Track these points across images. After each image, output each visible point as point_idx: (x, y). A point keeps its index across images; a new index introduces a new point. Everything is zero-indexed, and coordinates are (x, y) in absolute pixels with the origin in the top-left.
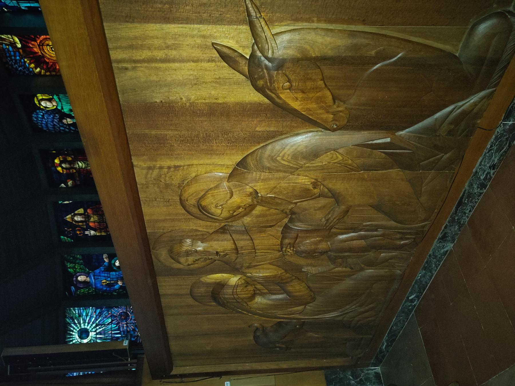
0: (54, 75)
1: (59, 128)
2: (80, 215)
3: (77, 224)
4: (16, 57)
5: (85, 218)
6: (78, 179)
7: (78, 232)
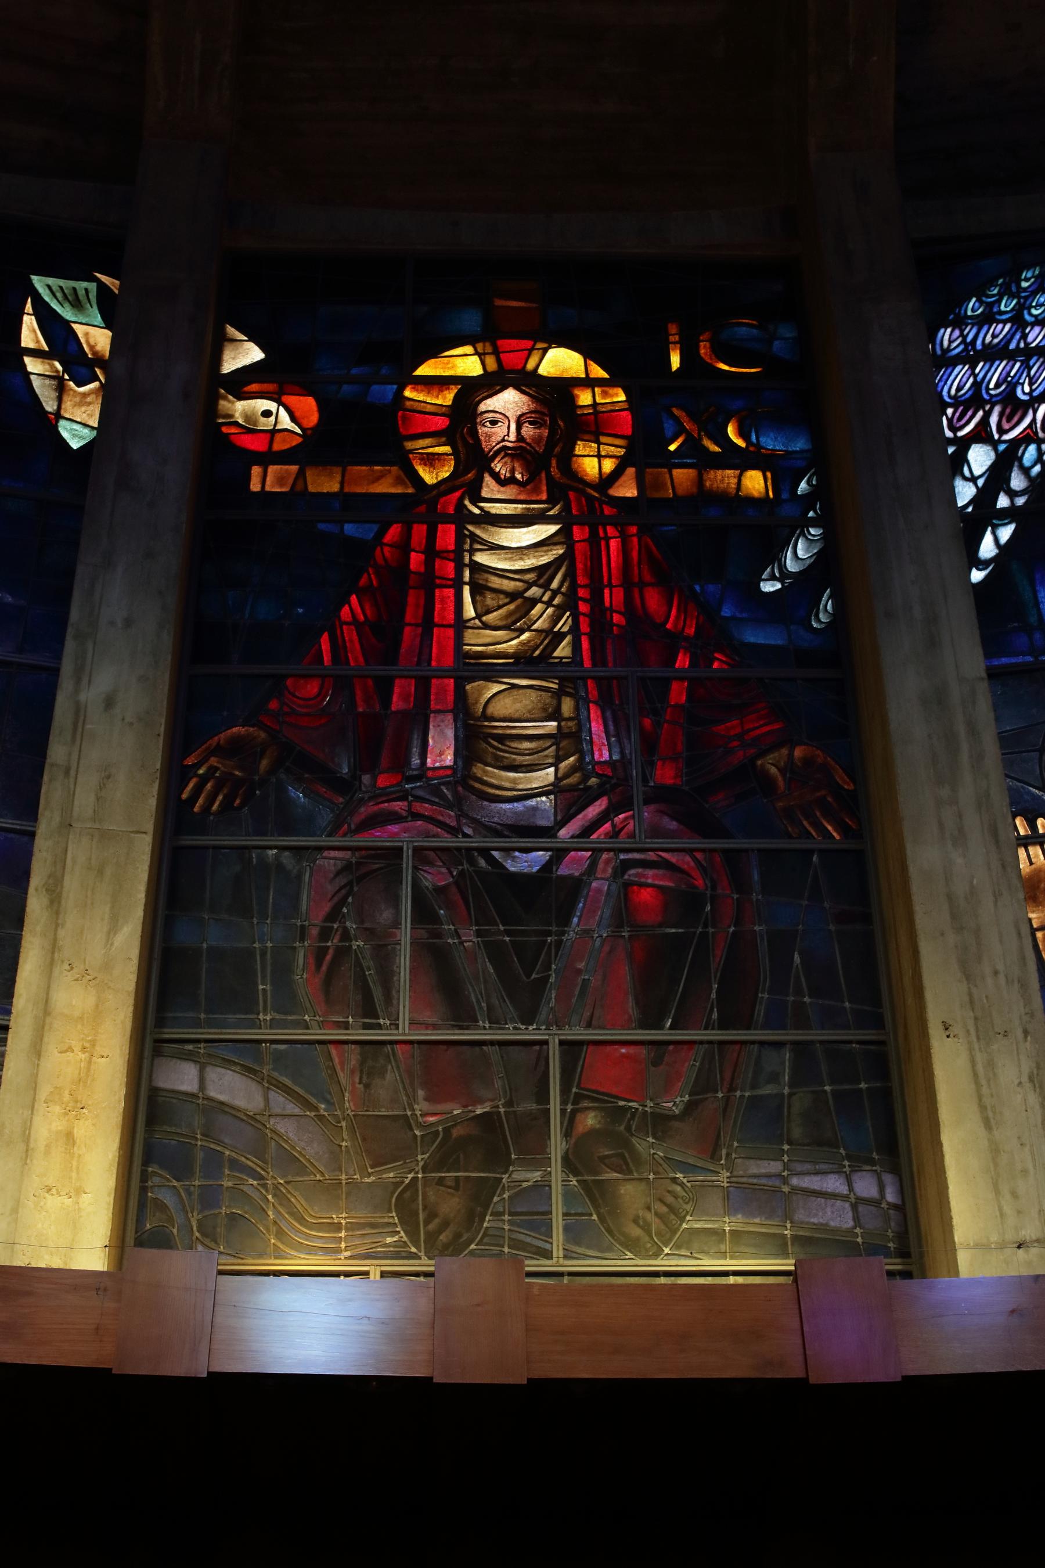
1: (982, 435)
6: (325, 483)
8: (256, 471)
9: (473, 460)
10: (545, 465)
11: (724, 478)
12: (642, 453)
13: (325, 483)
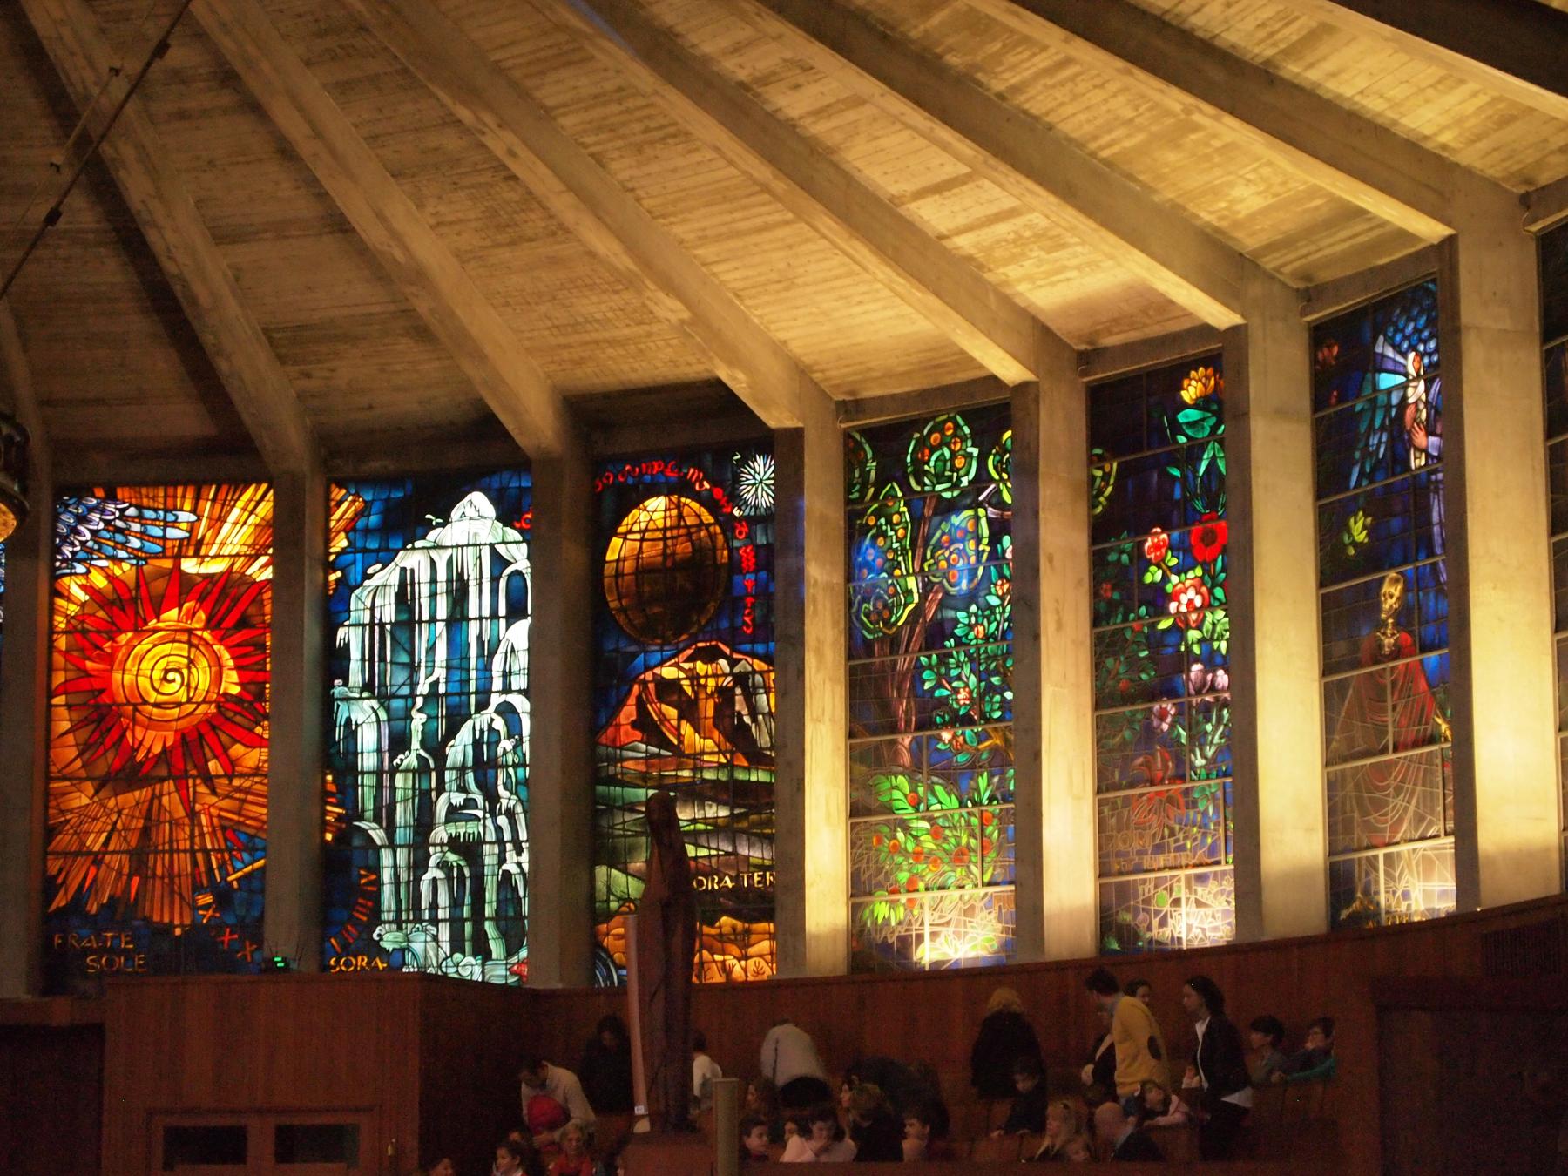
0: (51, 642)
4: (141, 539)
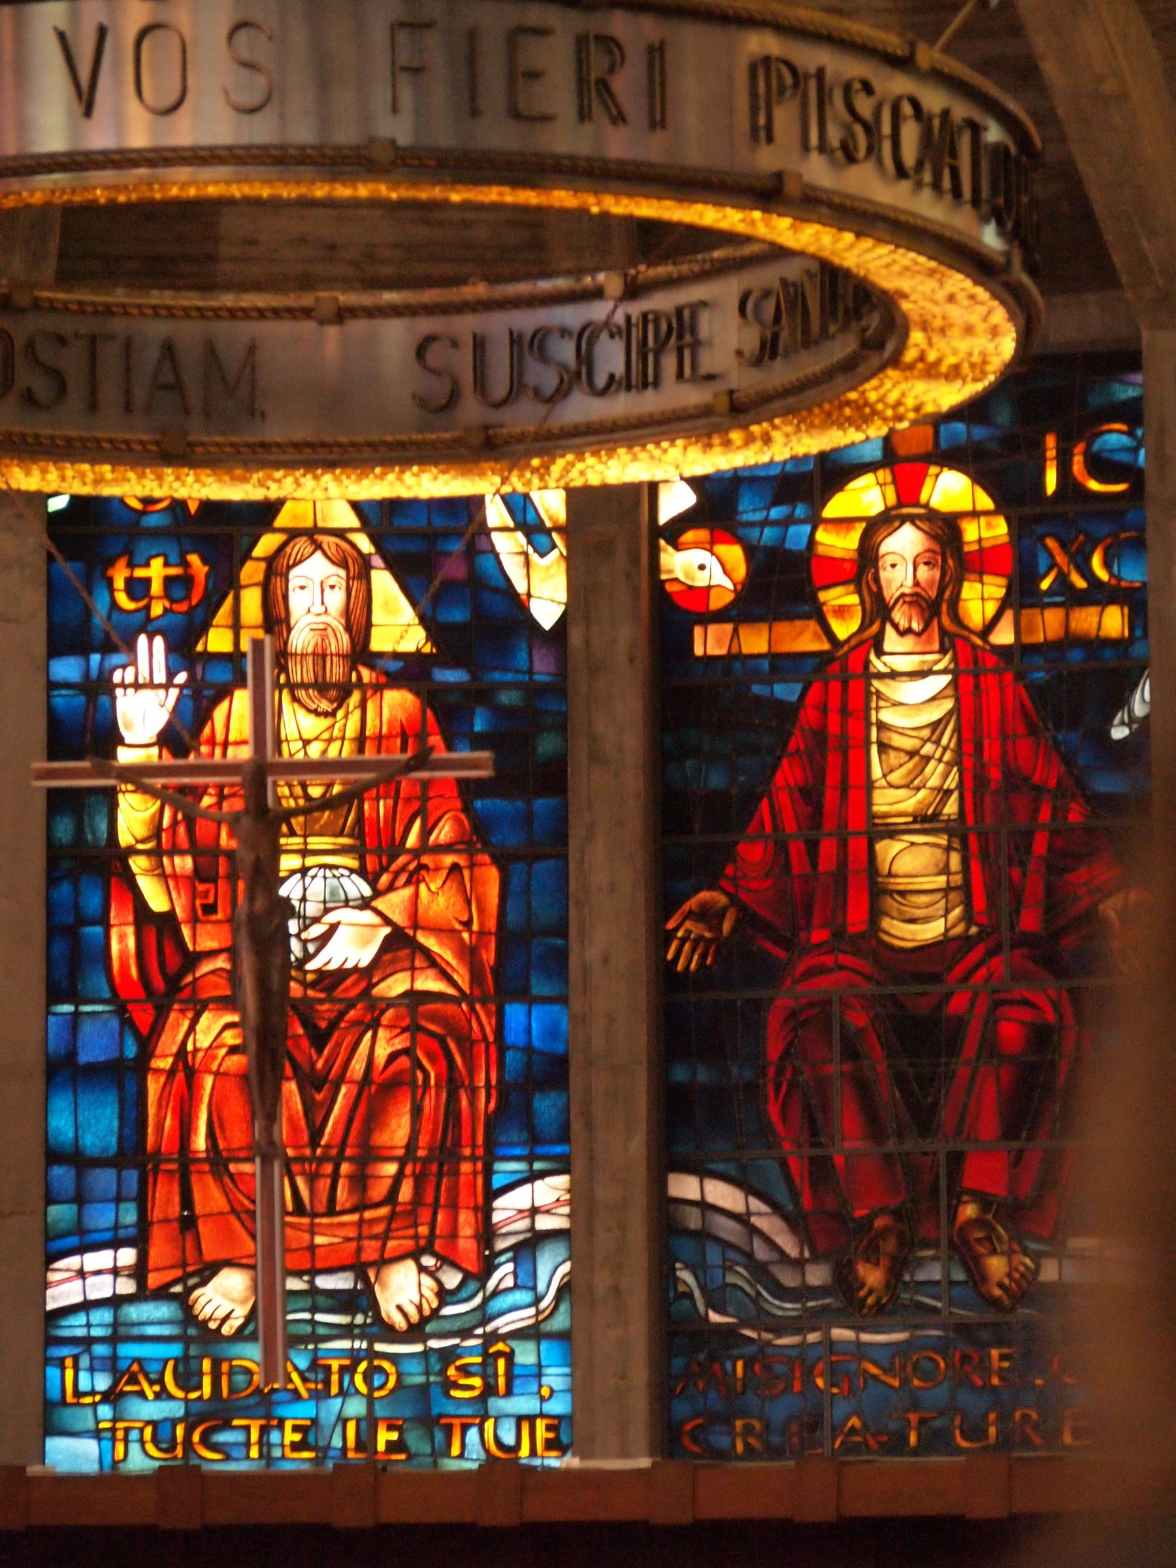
2: (358, 621)
3: (251, 572)
5: (320, 656)
6: (755, 642)
7: (156, 571)
8: (698, 631)
9: (878, 610)
10: (936, 608)
11: (1085, 620)
12: (1021, 597)
13: (755, 642)
